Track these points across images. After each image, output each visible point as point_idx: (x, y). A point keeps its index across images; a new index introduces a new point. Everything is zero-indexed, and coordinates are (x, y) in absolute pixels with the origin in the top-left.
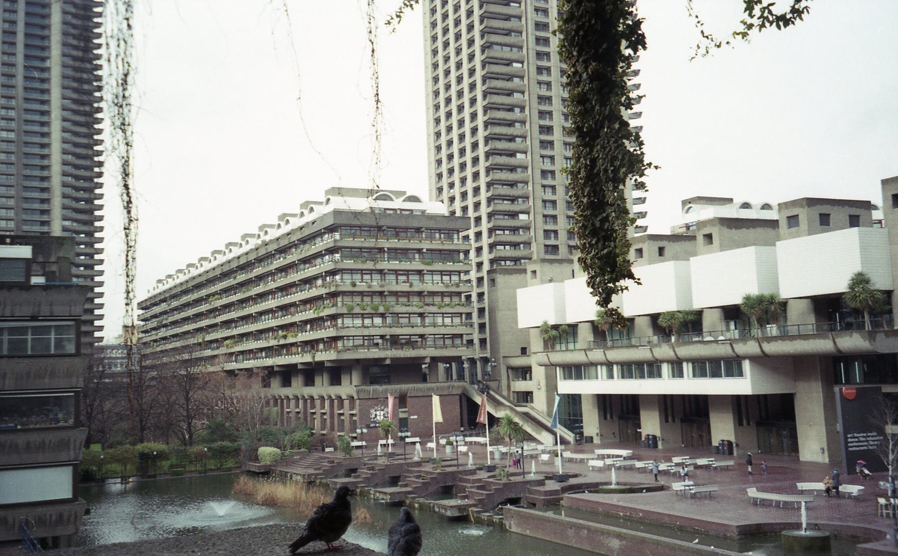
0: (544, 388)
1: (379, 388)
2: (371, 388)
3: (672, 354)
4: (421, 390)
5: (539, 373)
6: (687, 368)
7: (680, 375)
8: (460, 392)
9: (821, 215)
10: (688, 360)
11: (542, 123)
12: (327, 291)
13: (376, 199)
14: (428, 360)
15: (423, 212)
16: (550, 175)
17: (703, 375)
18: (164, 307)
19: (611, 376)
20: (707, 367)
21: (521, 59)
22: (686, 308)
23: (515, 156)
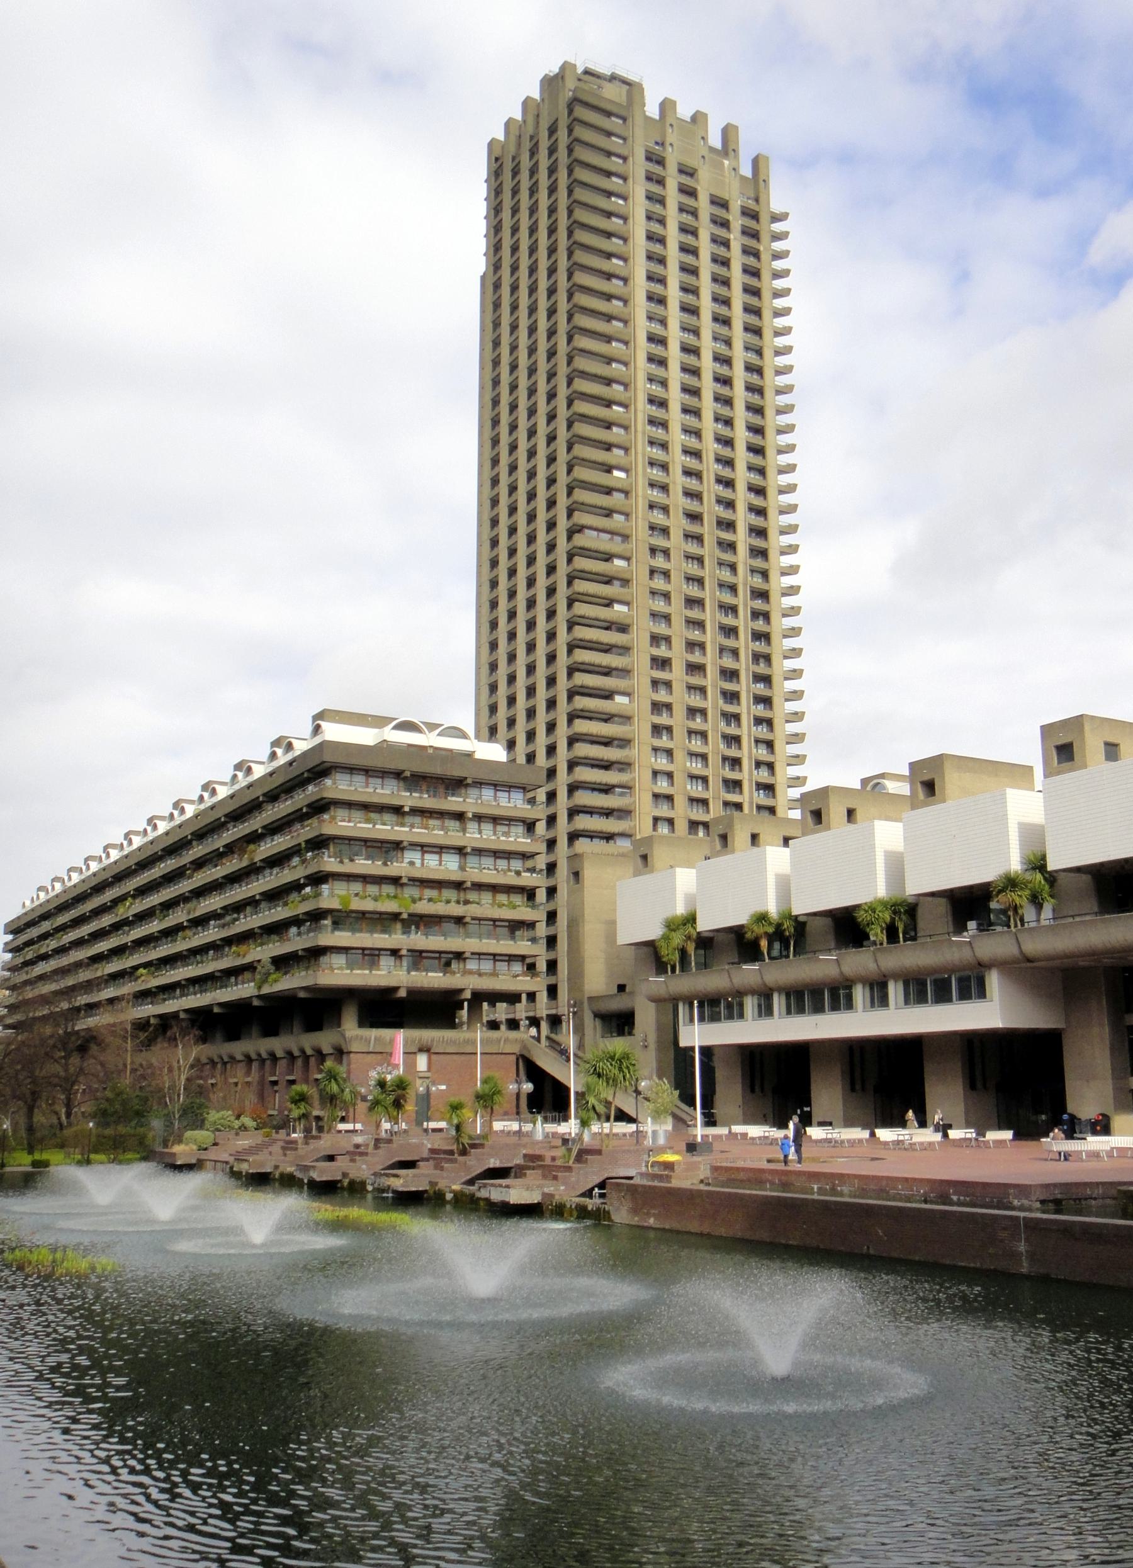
0: (652, 1046)
1: (386, 1033)
2: (374, 1033)
3: (872, 966)
4: (454, 1042)
5: (646, 1019)
6: (895, 991)
7: (884, 1001)
8: (516, 1049)
9: (1107, 744)
10: (896, 976)
11: (656, 652)
12: (309, 871)
13: (395, 728)
14: (467, 995)
15: (469, 755)
16: (665, 732)
17: (921, 999)
18: (46, 926)
19: (766, 1010)
20: (928, 987)
21: (628, 554)
22: (897, 895)
23: (613, 699)
